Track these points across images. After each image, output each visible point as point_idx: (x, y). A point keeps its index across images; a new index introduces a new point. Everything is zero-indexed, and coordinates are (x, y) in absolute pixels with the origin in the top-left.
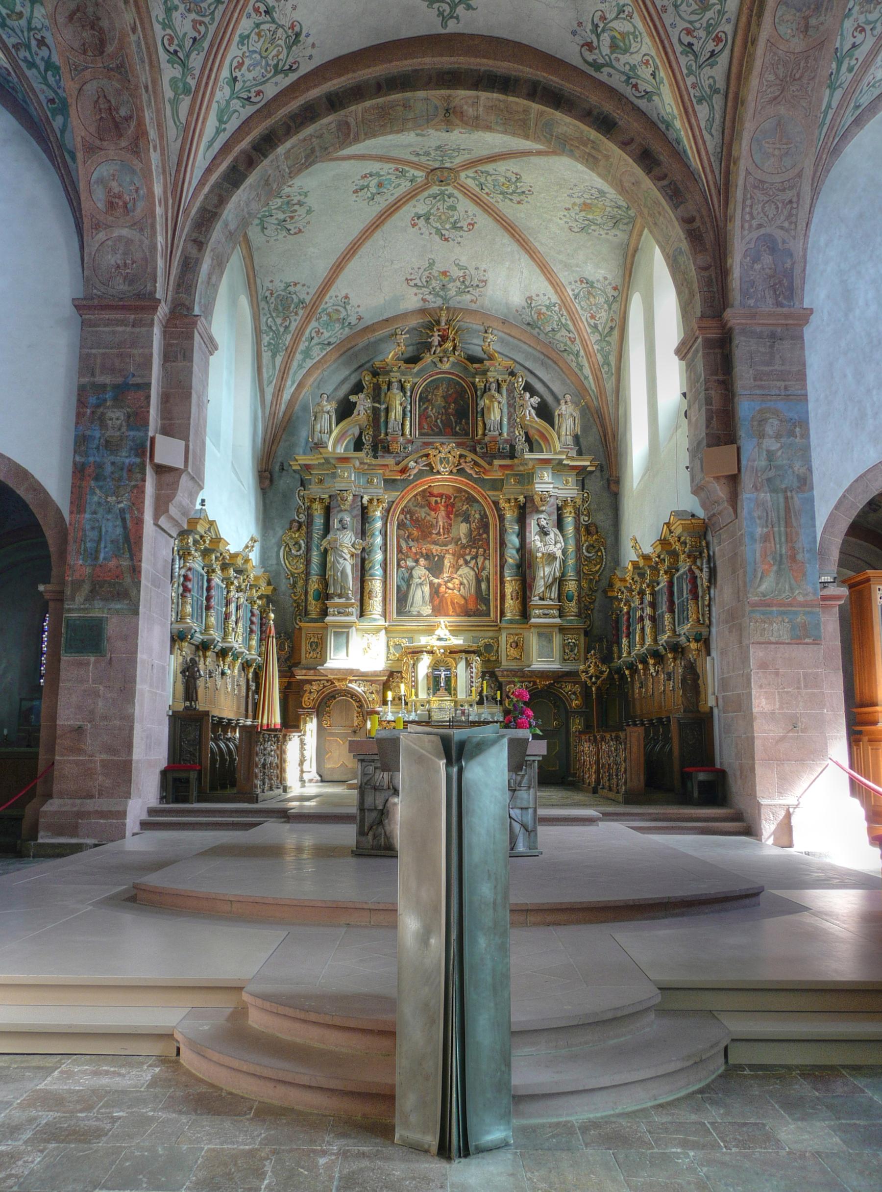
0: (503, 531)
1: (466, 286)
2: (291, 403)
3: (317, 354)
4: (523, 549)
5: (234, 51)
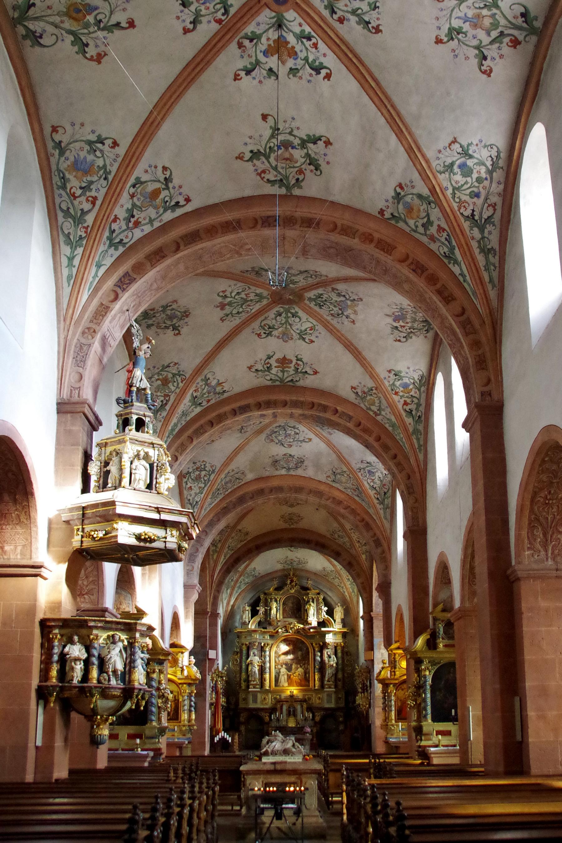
0: (315, 655)
1: (299, 562)
2: (233, 606)
3: (243, 587)
4: (322, 662)
5: (230, 541)
